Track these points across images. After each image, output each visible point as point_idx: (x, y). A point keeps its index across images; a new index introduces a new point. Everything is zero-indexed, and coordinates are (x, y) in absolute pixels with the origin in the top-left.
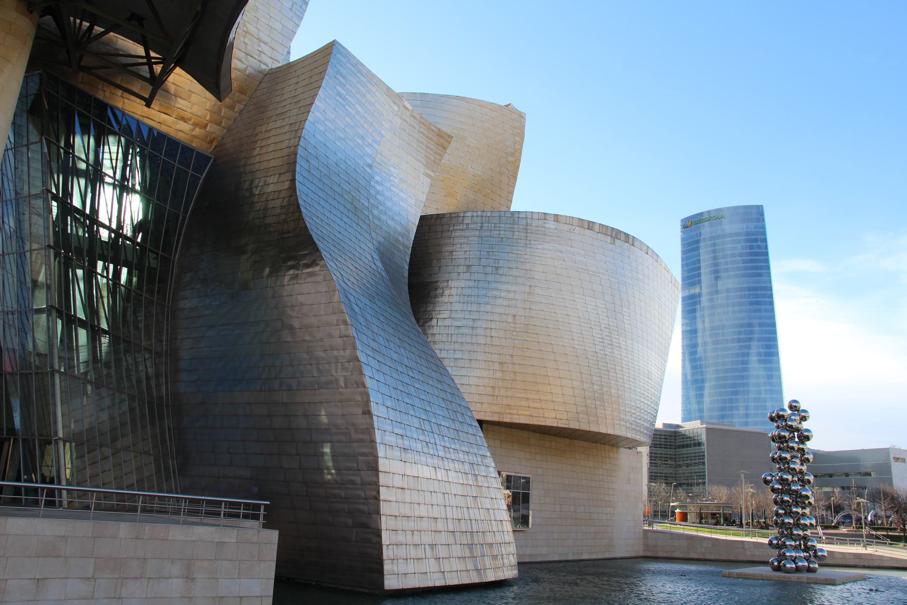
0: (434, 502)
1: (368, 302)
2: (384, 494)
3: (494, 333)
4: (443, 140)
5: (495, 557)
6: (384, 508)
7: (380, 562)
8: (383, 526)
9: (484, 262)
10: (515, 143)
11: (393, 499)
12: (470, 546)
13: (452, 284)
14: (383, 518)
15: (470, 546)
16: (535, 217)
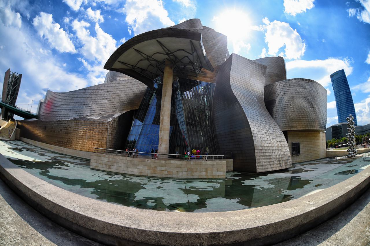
0: (270, 151)
1: (251, 107)
2: (256, 151)
3: (287, 109)
4: (265, 68)
5: (286, 163)
6: (256, 154)
7: (256, 166)
8: (256, 158)
9: (281, 93)
10: (283, 64)
11: (259, 152)
12: (279, 161)
13: (276, 99)
14: (256, 157)
15: (279, 161)
16: (290, 80)
